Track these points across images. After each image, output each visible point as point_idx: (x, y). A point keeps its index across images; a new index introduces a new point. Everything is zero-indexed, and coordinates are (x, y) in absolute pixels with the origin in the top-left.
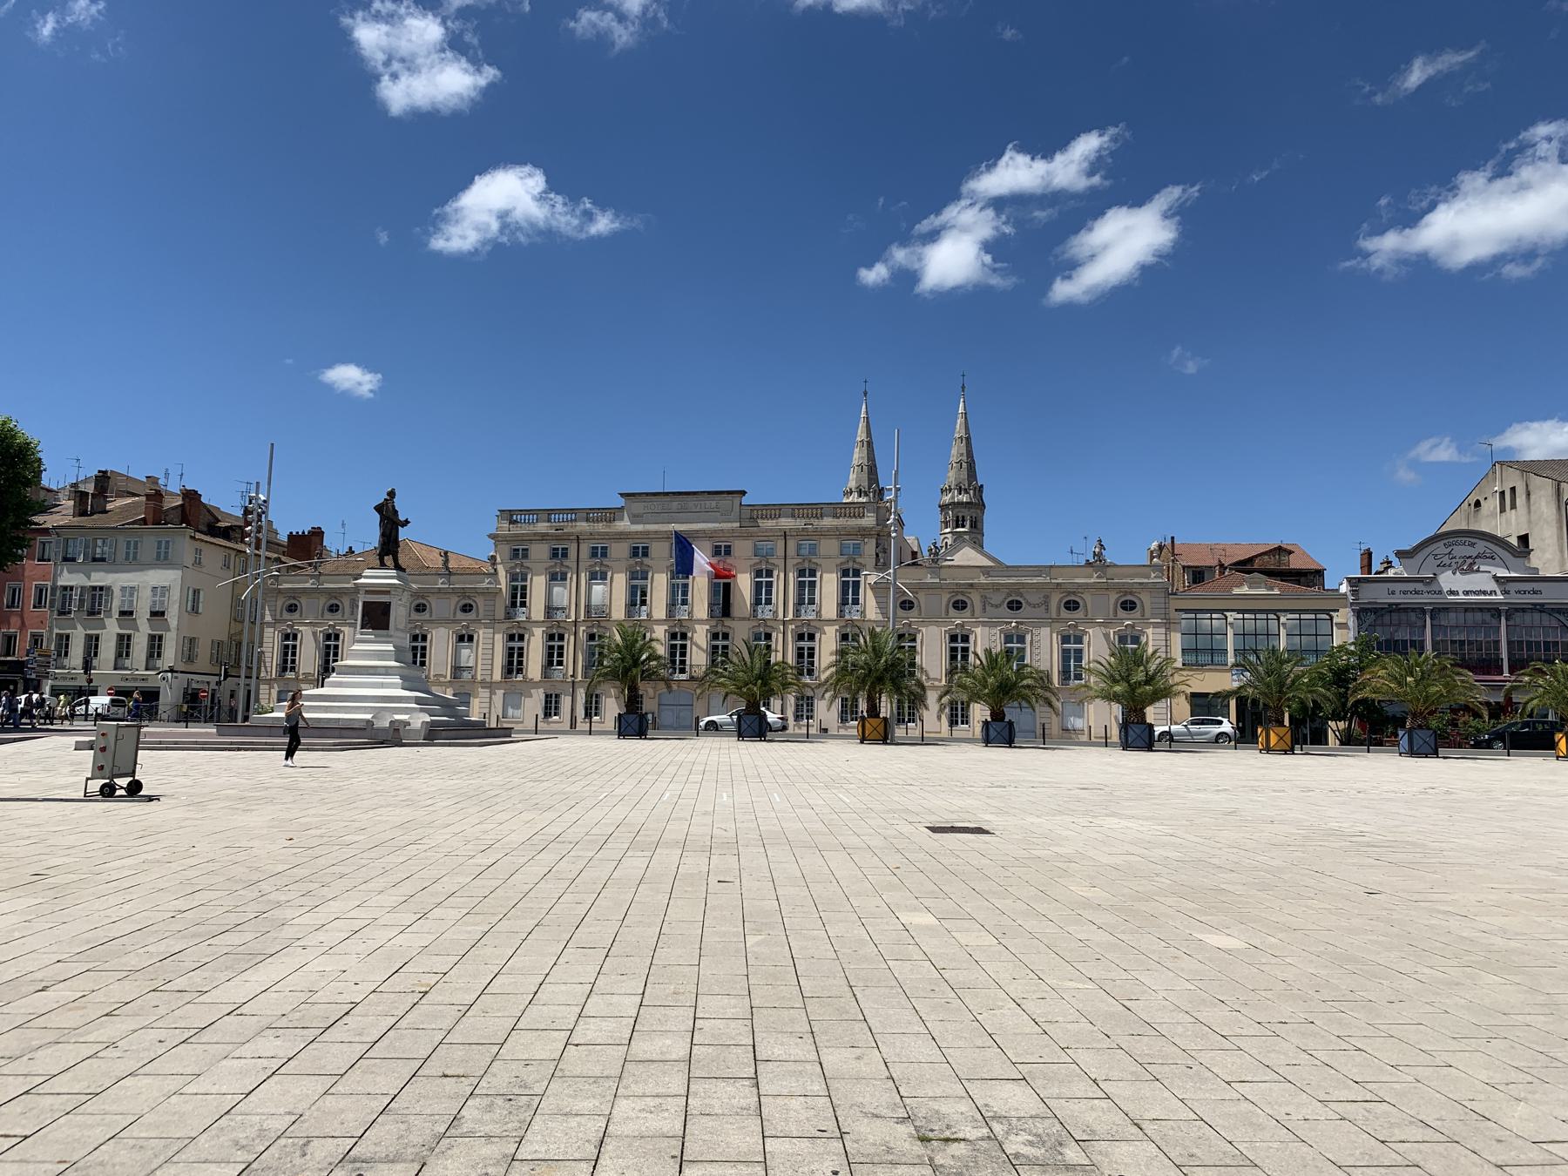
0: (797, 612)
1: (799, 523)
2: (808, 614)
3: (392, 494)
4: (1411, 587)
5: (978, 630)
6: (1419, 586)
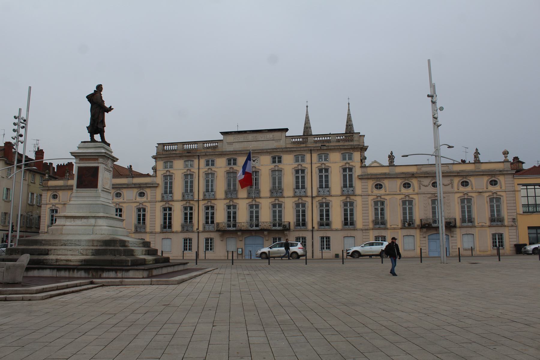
3: (99, 88)
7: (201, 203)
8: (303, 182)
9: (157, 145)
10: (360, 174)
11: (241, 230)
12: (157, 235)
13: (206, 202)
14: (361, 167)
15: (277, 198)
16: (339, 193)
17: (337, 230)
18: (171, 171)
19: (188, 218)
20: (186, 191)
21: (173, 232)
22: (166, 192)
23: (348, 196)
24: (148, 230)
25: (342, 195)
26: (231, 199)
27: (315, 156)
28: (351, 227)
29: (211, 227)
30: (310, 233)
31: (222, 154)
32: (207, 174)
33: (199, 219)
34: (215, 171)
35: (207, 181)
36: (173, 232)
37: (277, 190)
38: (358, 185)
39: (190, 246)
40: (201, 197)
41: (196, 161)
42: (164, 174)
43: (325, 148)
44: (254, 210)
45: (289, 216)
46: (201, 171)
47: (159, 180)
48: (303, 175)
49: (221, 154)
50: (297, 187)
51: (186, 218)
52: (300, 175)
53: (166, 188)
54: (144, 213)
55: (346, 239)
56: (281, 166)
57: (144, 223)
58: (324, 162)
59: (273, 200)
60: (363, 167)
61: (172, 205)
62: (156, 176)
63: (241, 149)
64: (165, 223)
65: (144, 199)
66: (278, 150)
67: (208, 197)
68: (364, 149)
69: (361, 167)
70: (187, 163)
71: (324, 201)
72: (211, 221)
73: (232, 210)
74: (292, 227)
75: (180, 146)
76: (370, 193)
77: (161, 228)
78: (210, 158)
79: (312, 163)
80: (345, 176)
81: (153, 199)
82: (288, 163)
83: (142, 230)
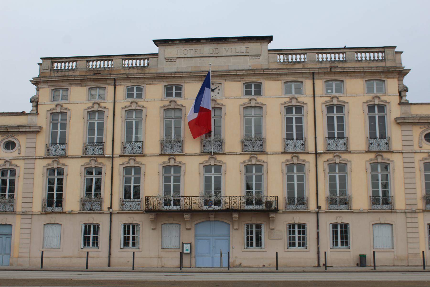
7: (118, 162)
8: (300, 128)
9: (41, 61)
10: (398, 116)
11: (190, 211)
12: (35, 218)
13: (126, 160)
14: (400, 104)
15: (254, 154)
16: (363, 147)
17: (361, 212)
18: (65, 106)
19: (93, 189)
20: (91, 141)
21: (65, 213)
22: (54, 143)
23: (379, 153)
24: (19, 208)
25: (369, 152)
26: (172, 156)
27: (320, 84)
28: (385, 206)
29: (134, 205)
30: (314, 217)
31: (157, 78)
32: (129, 112)
33: (113, 190)
34: (143, 107)
35: (129, 124)
36: (65, 213)
37: (254, 143)
38: (396, 135)
39: (96, 238)
40: (118, 151)
41: (110, 89)
42: (51, 110)
43: (338, 70)
44: (213, 174)
45: (275, 187)
46: (119, 106)
47: (43, 120)
48: (299, 115)
49: (155, 78)
50: (289, 137)
51: (89, 189)
52: (294, 115)
53: (54, 134)
54: (12, 178)
55: (377, 228)
56: (260, 100)
57: (12, 196)
58: (334, 94)
59: (247, 157)
60: (403, 103)
61: (64, 164)
62: (37, 114)
63: (189, 70)
64: (50, 196)
65: (13, 153)
66: (256, 72)
67: (129, 151)
68: (401, 73)
69: (400, 104)
70: (93, 92)
71: (337, 160)
72: (134, 195)
73: (172, 175)
74: (281, 207)
75: (82, 64)
76: (416, 148)
77: (44, 206)
78: (135, 84)
79: (315, 96)
80: (372, 119)
81: (32, 154)
82: (274, 94)
83: (8, 209)
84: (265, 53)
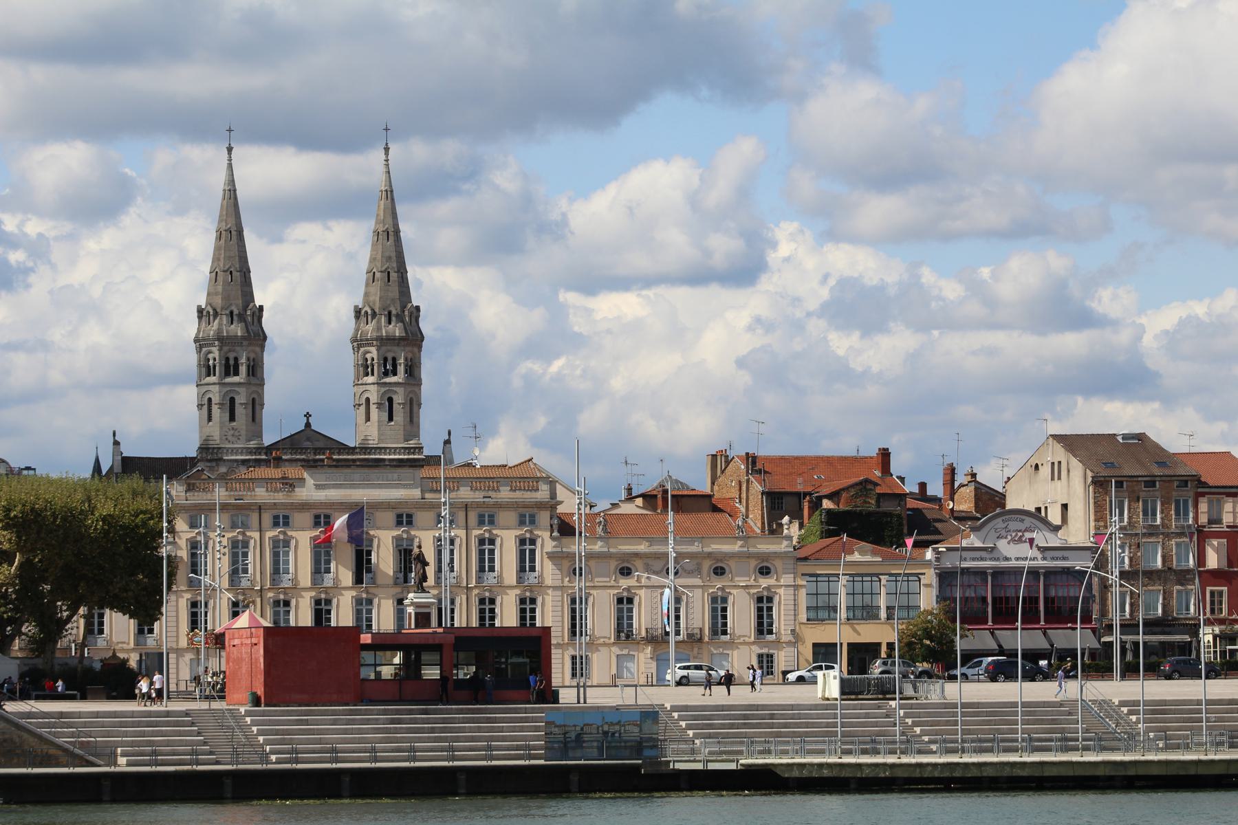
0: (479, 579)
1: (478, 496)
2: (490, 579)
4: (977, 554)
5: (642, 592)
6: (984, 554)
84: (418, 480)
